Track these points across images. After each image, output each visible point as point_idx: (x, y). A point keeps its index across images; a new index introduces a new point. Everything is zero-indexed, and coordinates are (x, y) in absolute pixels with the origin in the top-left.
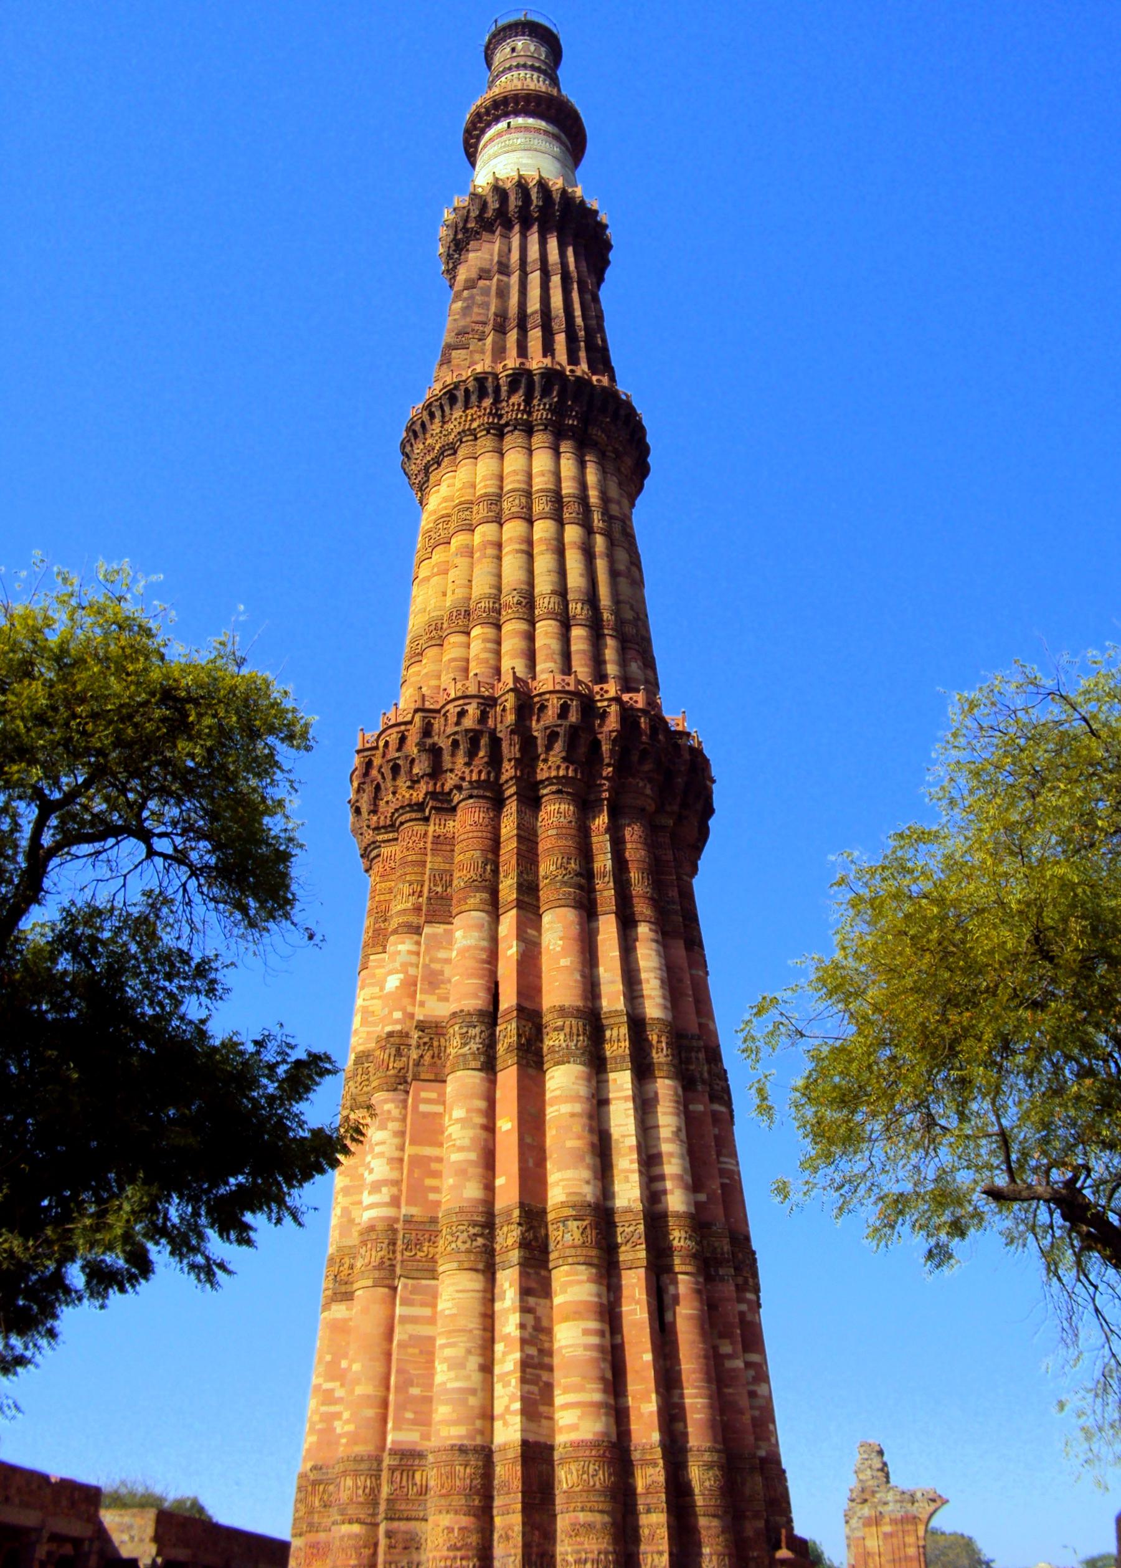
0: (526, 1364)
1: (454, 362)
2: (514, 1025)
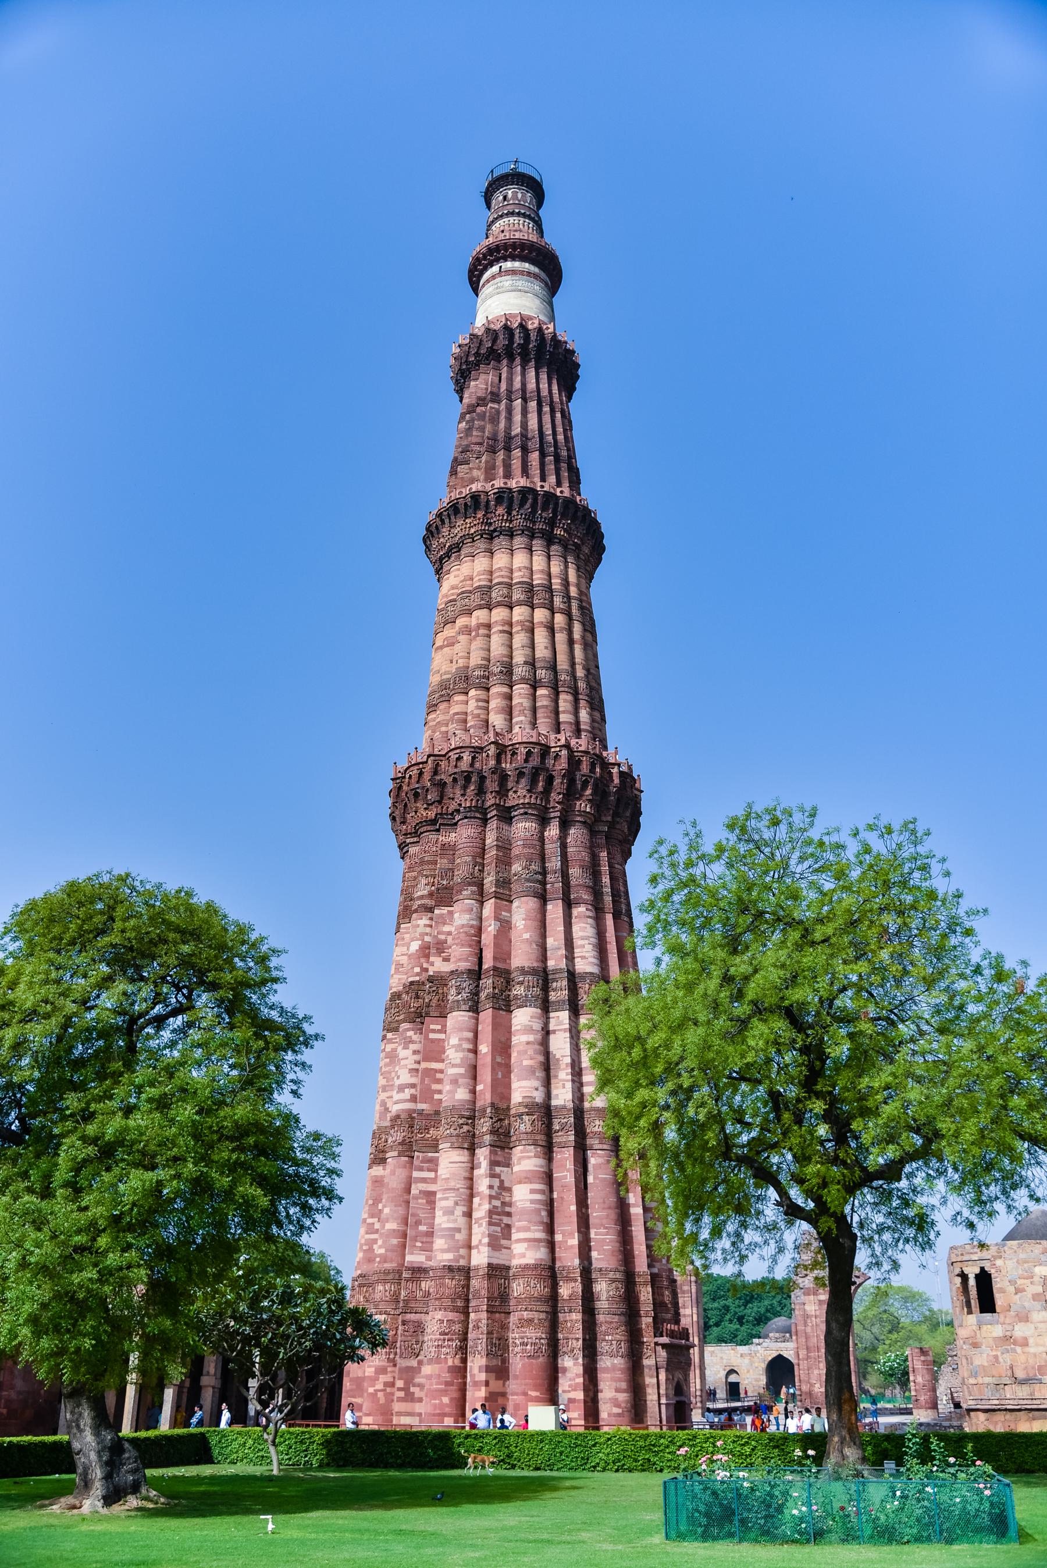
1: (460, 475)
2: (491, 981)
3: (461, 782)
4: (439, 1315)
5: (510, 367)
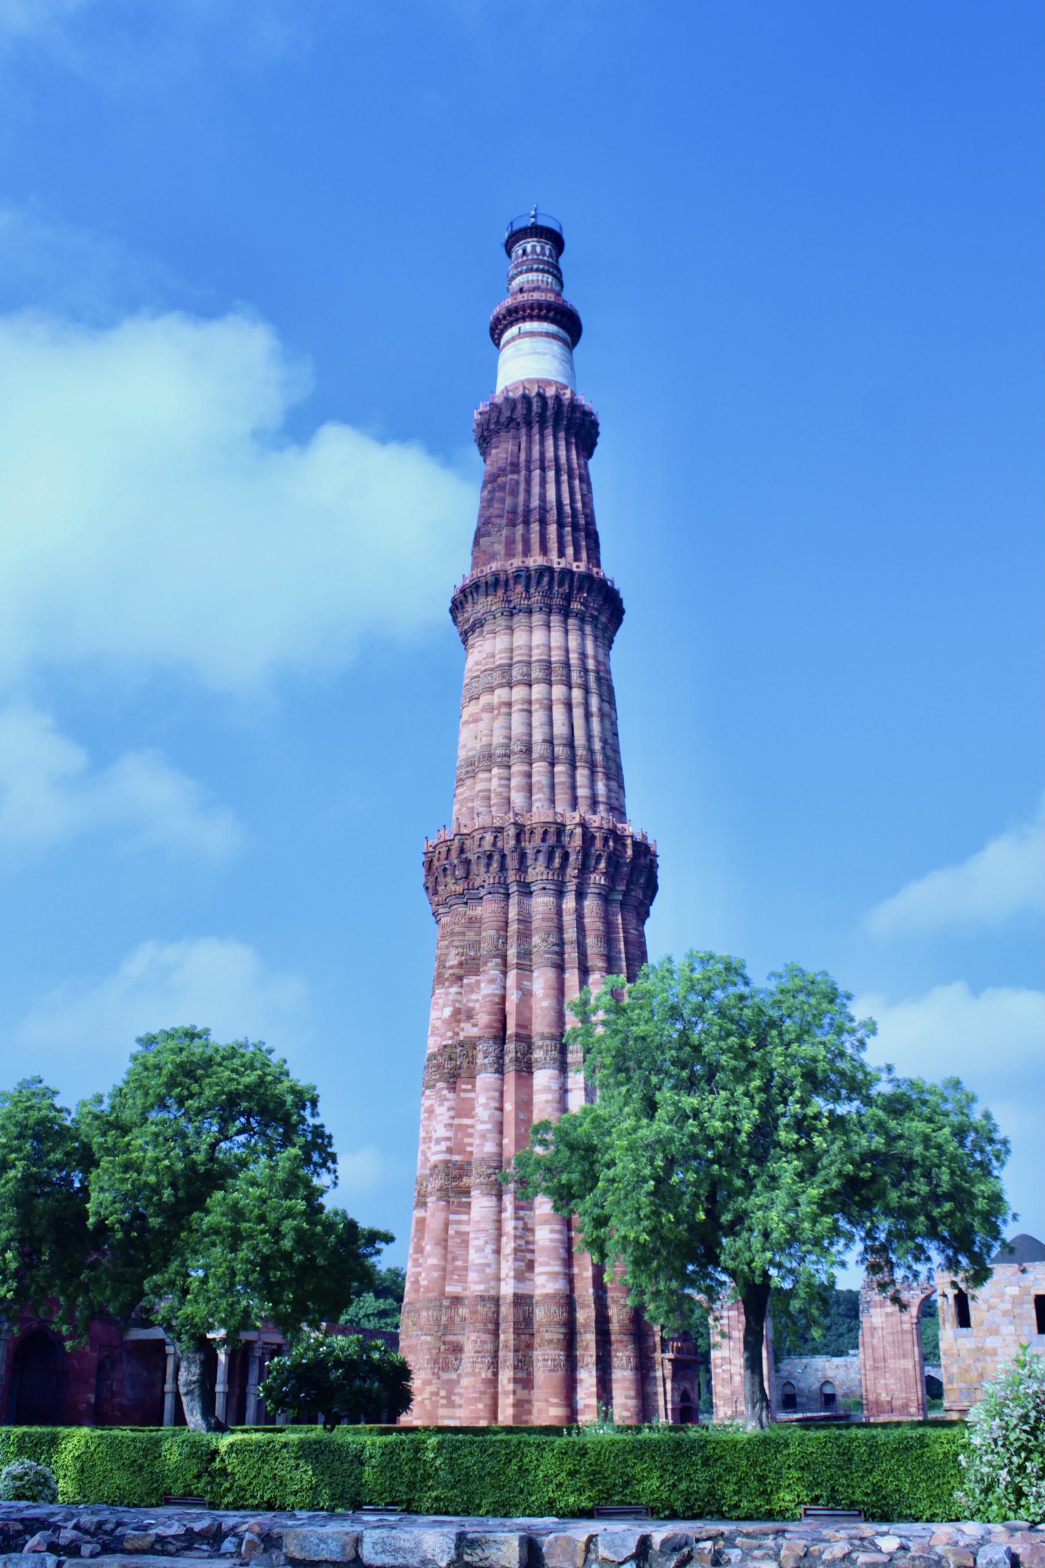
0: (516, 1250)
3: (484, 861)
4: (473, 1336)
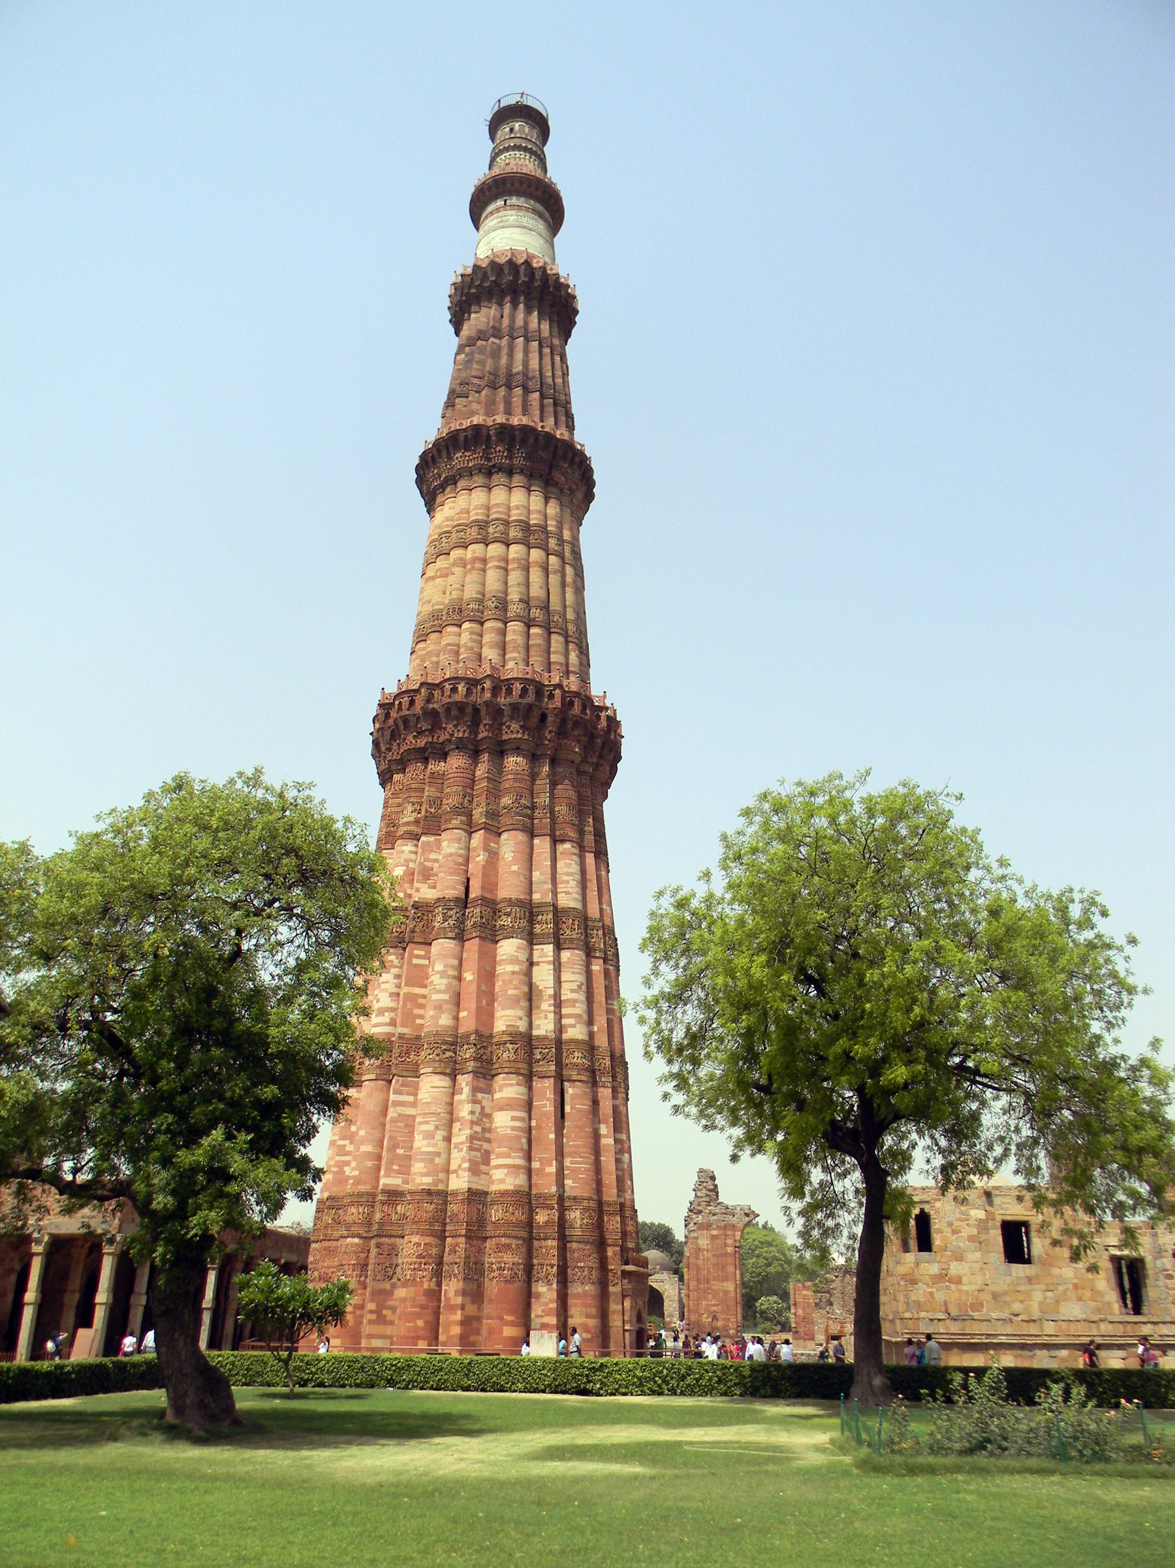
1: (458, 407)
4: (416, 1239)
5: (515, 305)
